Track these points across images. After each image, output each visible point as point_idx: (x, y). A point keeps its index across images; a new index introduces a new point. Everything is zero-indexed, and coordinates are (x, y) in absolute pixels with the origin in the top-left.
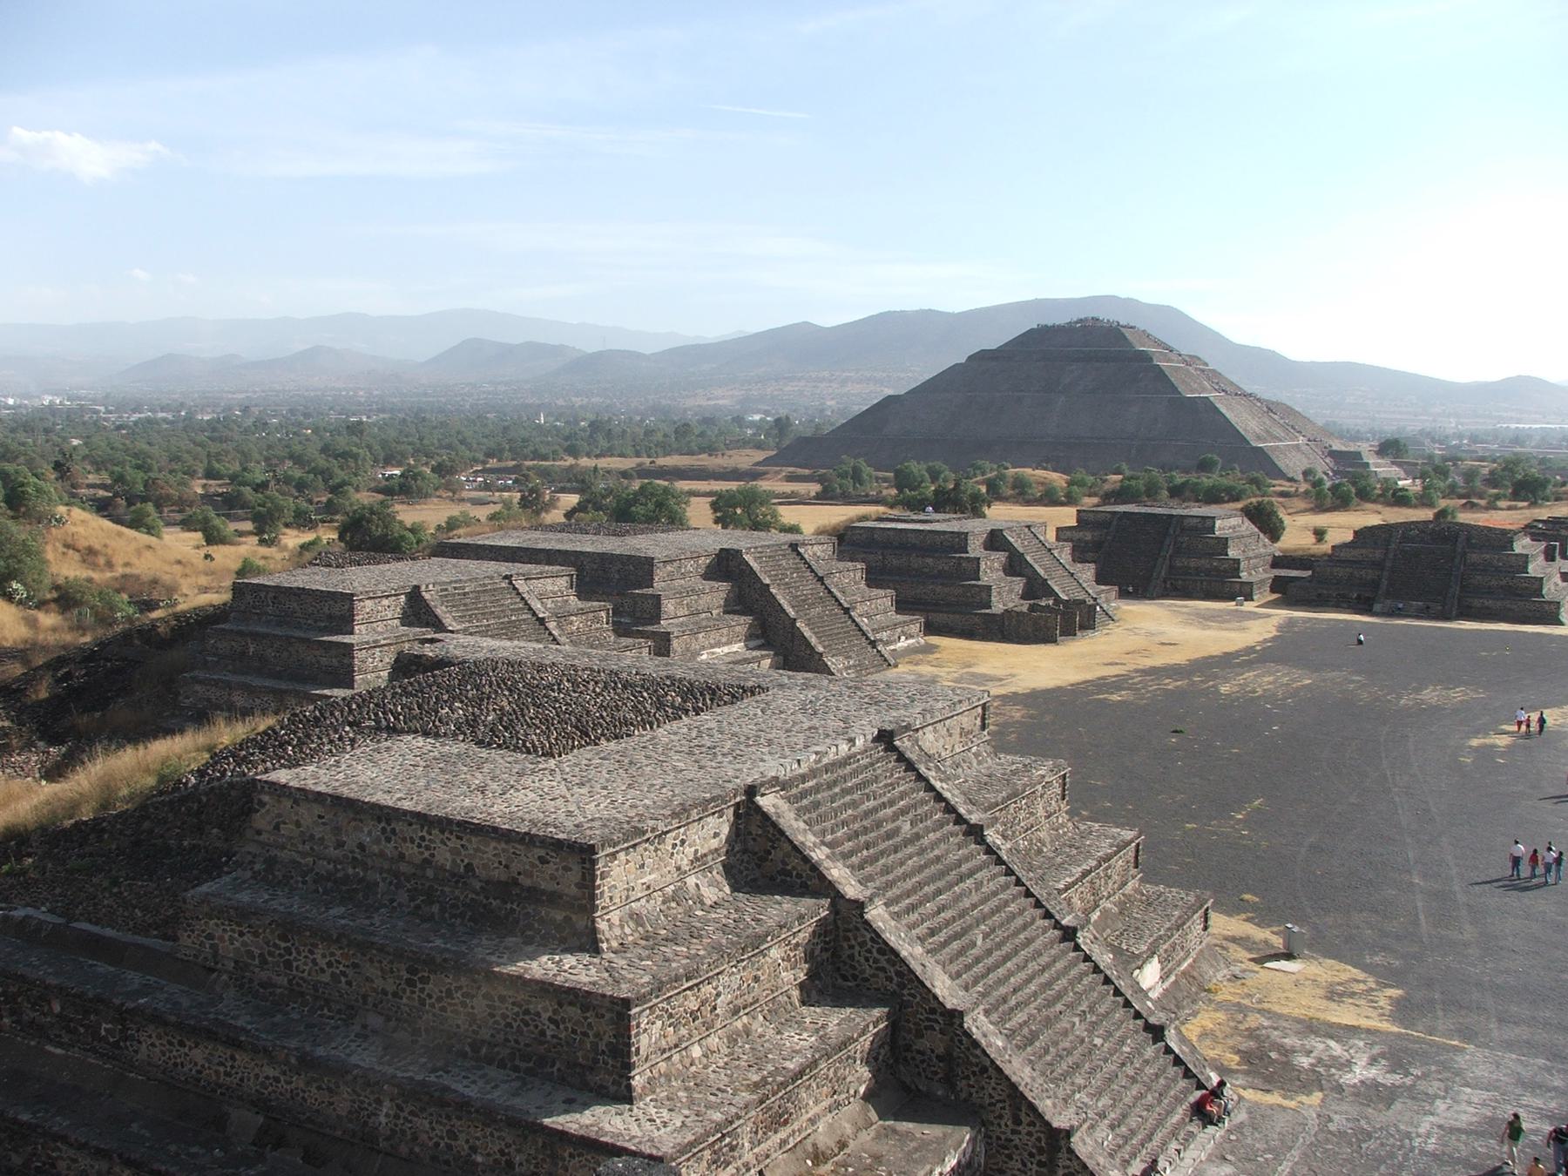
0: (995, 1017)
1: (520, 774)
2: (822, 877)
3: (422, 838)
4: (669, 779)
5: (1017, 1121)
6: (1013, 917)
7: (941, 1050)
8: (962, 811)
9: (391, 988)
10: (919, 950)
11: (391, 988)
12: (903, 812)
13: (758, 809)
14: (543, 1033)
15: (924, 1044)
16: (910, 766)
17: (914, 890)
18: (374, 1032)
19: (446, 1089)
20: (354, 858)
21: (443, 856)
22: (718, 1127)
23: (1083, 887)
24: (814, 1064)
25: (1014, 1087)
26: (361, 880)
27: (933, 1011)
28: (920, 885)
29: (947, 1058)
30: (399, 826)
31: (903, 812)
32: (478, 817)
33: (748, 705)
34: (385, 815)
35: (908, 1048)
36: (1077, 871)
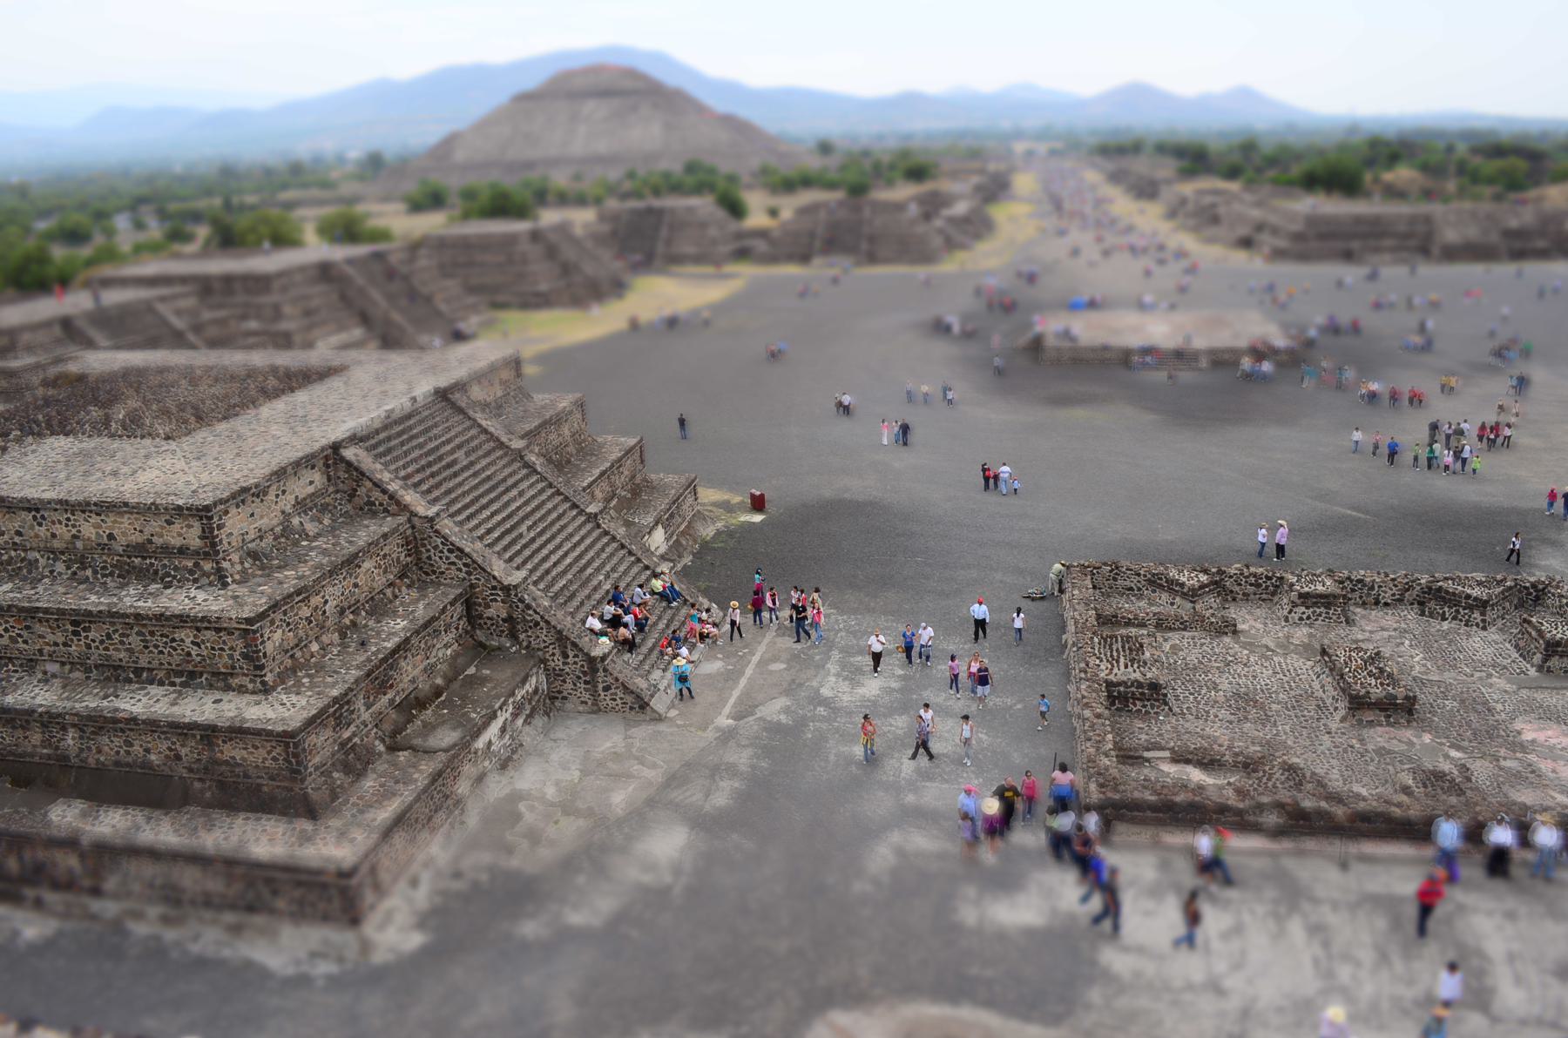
0: (542, 586)
1: (147, 457)
2: (398, 503)
3: (68, 519)
4: (268, 446)
5: (566, 656)
6: (549, 512)
7: (504, 615)
8: (504, 439)
9: (61, 640)
10: (479, 545)
11: (61, 640)
12: (459, 447)
13: (343, 459)
14: (189, 654)
15: (491, 612)
16: (461, 411)
17: (472, 502)
18: (54, 676)
19: (116, 710)
20: (15, 544)
22: (335, 700)
23: (604, 485)
24: (407, 640)
25: (560, 632)
26: (23, 560)
27: (494, 588)
28: (477, 499)
29: (510, 619)
31: (459, 447)
32: (111, 496)
33: (336, 383)
35: (480, 616)
36: (597, 472)
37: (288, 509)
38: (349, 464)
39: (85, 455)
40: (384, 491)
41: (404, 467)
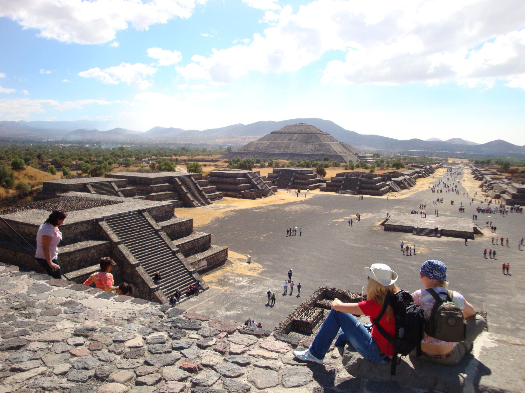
8: (154, 227)
21: (27, 231)
25: (143, 280)
30: (19, 225)
33: (115, 206)
34: (17, 223)
37: (77, 234)
38: (99, 225)
39: (38, 213)
40: (106, 233)
41: (117, 229)
